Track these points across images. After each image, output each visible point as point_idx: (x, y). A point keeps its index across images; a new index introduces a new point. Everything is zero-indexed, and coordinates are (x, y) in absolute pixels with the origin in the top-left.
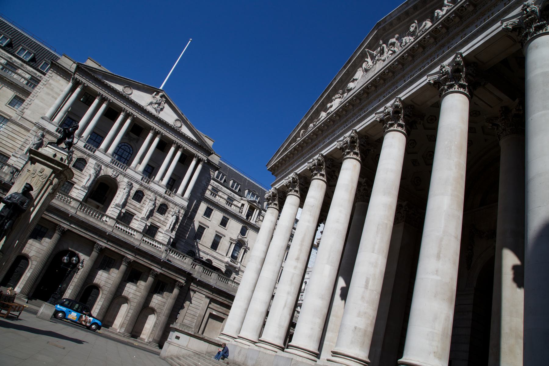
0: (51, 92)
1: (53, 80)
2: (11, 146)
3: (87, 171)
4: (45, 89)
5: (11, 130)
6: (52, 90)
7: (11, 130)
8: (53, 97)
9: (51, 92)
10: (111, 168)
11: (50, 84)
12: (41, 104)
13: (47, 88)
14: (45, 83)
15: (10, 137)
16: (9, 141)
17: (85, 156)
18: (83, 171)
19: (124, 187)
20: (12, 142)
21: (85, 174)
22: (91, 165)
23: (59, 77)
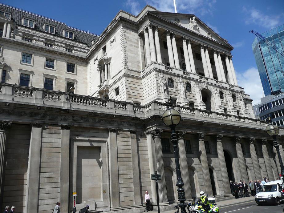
0: (132, 43)
1: (128, 33)
2: (136, 94)
3: (195, 91)
4: (127, 42)
5: (129, 82)
6: (131, 41)
7: (129, 82)
8: (135, 46)
9: (132, 43)
10: (202, 83)
11: (128, 37)
12: (132, 55)
13: (128, 41)
14: (125, 37)
15: (132, 88)
16: (133, 91)
17: (188, 81)
18: (192, 92)
19: (215, 93)
20: (135, 91)
21: (194, 93)
22: (194, 85)
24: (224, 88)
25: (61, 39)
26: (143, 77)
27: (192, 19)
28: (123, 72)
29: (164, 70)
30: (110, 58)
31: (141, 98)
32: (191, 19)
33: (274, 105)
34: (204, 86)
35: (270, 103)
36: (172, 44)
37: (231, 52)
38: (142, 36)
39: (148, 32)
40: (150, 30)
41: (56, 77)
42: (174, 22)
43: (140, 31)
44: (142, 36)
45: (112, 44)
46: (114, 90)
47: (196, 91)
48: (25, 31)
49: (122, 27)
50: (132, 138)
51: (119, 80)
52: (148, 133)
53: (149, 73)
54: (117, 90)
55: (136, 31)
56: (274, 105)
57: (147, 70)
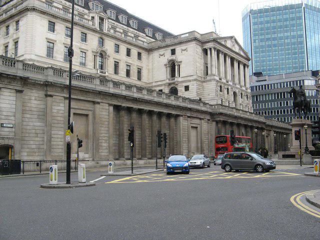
23: (198, 46)
24: (243, 90)
25: (131, 29)
26: (204, 82)
28: (195, 77)
29: (218, 80)
30: (181, 62)
33: (256, 90)
34: (234, 90)
35: (254, 87)
36: (222, 57)
41: (131, 64)
42: (223, 43)
43: (205, 47)
44: (205, 51)
45: (184, 52)
46: (184, 87)
47: (231, 93)
50: (208, 123)
51: (190, 81)
52: (213, 121)
53: (210, 80)
54: (187, 88)
55: (202, 46)
56: (256, 90)
57: (208, 78)
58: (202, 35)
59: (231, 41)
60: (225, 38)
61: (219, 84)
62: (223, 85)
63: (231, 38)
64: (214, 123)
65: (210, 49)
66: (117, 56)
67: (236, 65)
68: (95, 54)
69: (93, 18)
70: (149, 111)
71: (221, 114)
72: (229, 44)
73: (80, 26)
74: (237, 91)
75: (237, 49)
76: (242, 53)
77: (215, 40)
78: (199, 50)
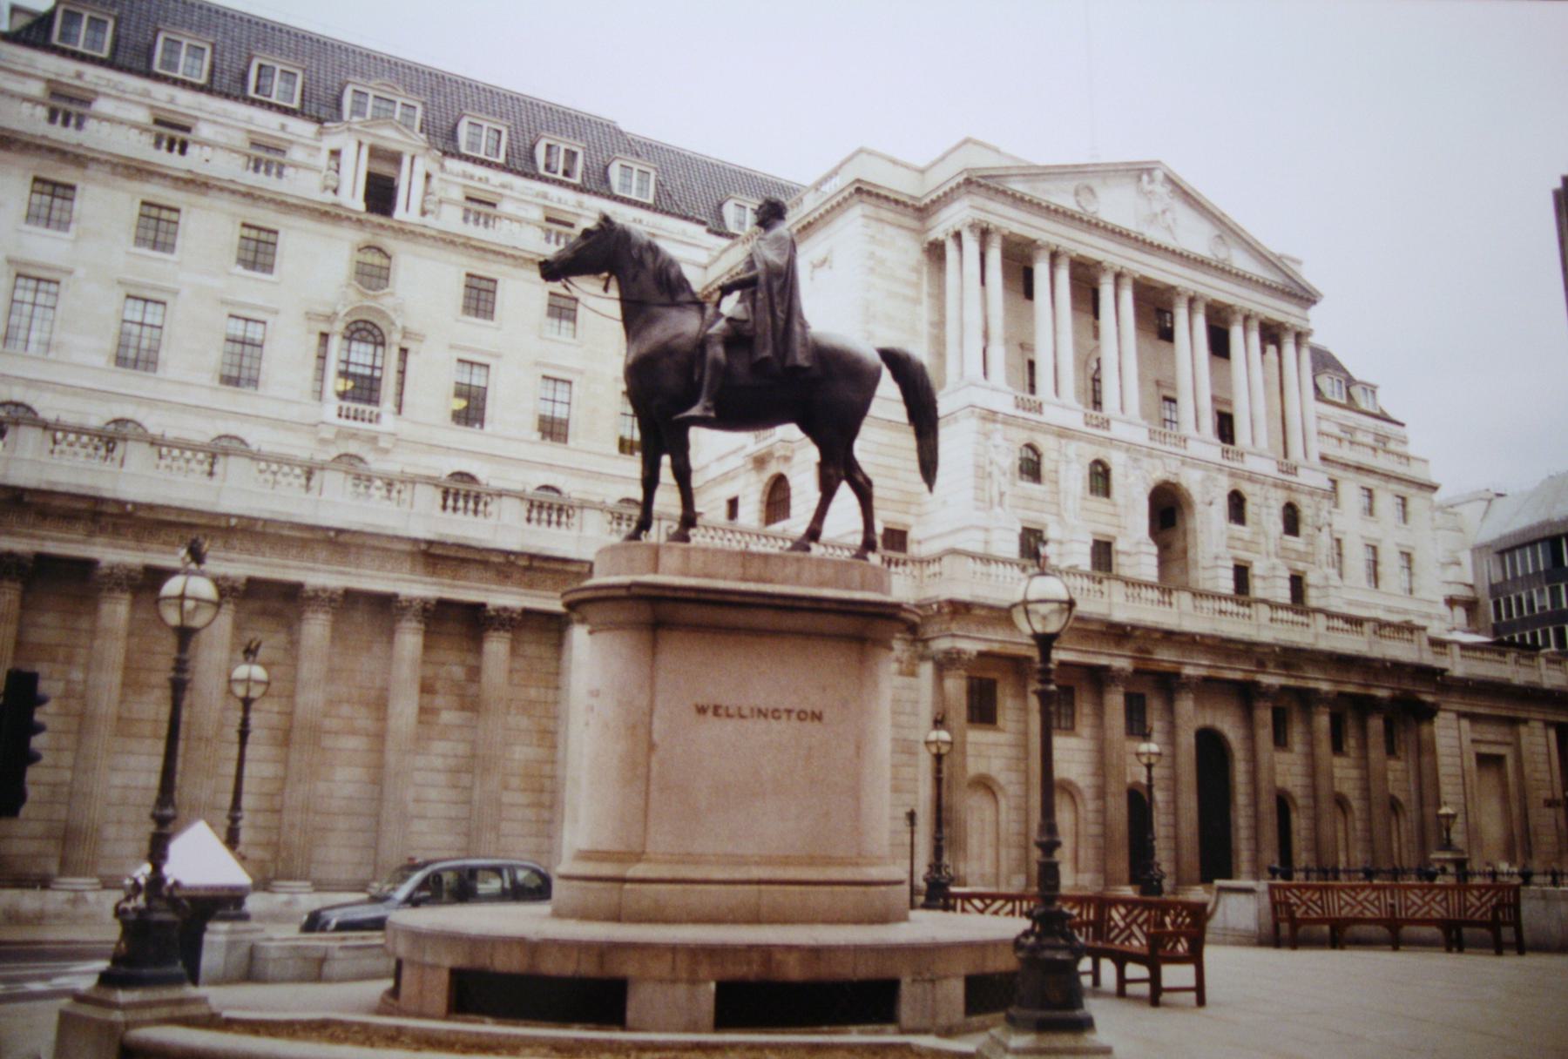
17: (1101, 453)
23: (889, 230)
27: (1152, 181)
31: (914, 509)
32: (1145, 178)
37: (1314, 313)
38: (936, 252)
39: (960, 246)
40: (971, 245)
43: (932, 236)
48: (472, 177)
49: (861, 221)
55: (922, 232)
58: (922, 172)
59: (1141, 192)
60: (1082, 174)
61: (1023, 437)
62: (1046, 444)
63: (1140, 171)
64: (927, 670)
65: (958, 236)
66: (477, 335)
67: (1191, 333)
68: (325, 328)
69: (335, 154)
70: (252, 582)
71: (960, 609)
72: (1117, 205)
73: (233, 192)
74: (1191, 481)
75: (1195, 237)
76: (1241, 261)
77: (973, 183)
78: (904, 250)
